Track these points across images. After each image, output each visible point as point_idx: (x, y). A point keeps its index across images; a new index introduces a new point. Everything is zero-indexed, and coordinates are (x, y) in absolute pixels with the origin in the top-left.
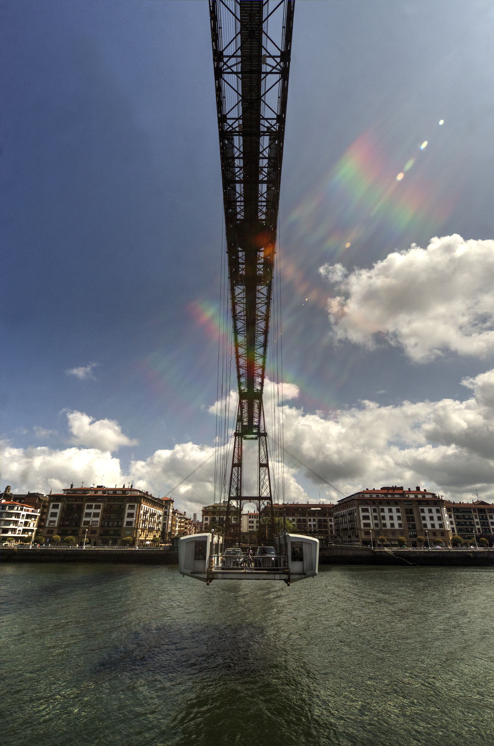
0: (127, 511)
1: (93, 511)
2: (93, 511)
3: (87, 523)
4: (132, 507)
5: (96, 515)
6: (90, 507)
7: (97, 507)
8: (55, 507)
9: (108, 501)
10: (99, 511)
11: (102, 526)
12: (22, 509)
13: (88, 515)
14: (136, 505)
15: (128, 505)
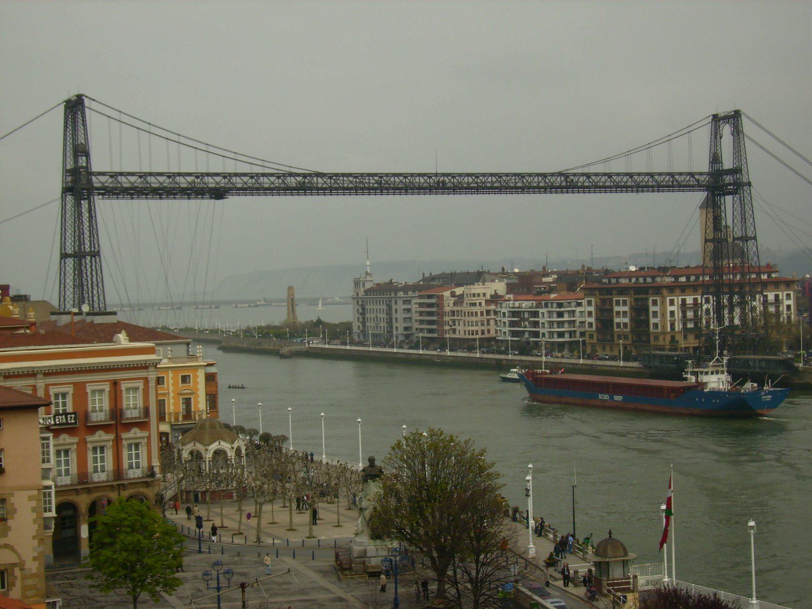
0: (652, 309)
1: (621, 309)
2: (621, 309)
3: (618, 325)
4: (655, 303)
5: (625, 313)
6: (618, 303)
7: (625, 303)
8: (589, 303)
9: (634, 294)
10: (626, 309)
11: (632, 331)
12: (579, 305)
13: (618, 313)
14: (658, 299)
15: (651, 299)
